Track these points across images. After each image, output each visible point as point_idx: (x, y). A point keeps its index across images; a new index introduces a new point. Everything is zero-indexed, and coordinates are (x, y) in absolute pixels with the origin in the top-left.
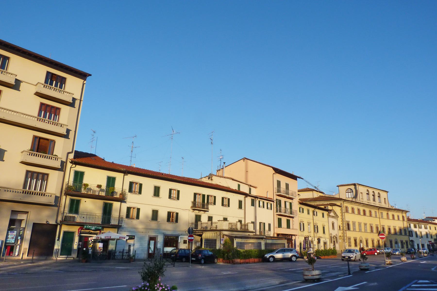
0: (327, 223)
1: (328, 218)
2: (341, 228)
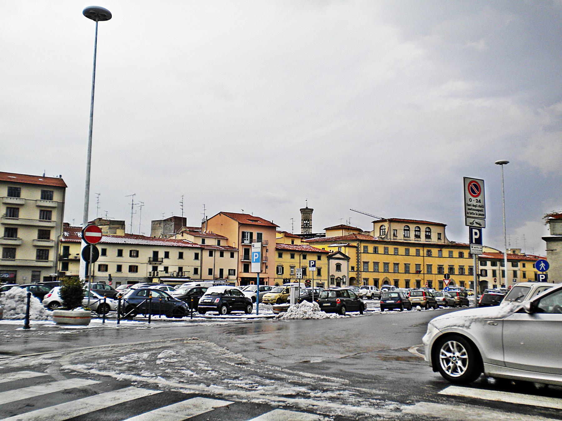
0: (327, 266)
1: (328, 260)
2: (355, 269)
